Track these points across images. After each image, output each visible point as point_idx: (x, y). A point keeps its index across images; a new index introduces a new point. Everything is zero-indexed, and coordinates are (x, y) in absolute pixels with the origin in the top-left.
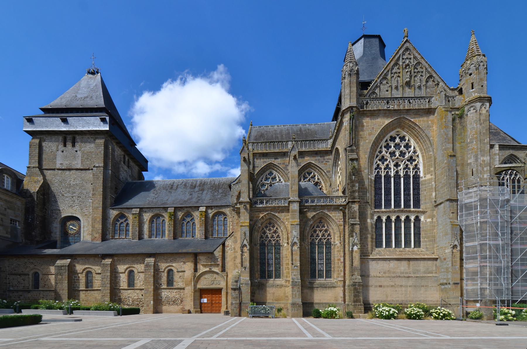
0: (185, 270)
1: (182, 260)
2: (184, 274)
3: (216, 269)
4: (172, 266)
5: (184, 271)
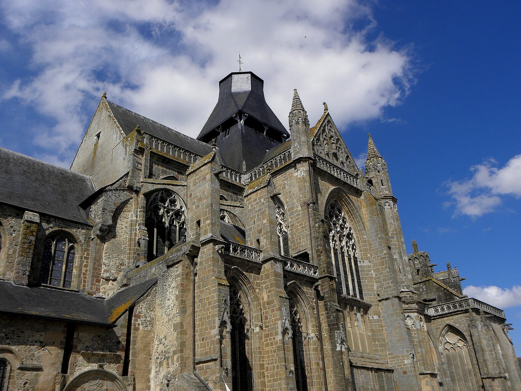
0: (42, 364)
1: (38, 336)
2: (37, 375)
3: (113, 369)
4: (11, 352)
5: (39, 369)
